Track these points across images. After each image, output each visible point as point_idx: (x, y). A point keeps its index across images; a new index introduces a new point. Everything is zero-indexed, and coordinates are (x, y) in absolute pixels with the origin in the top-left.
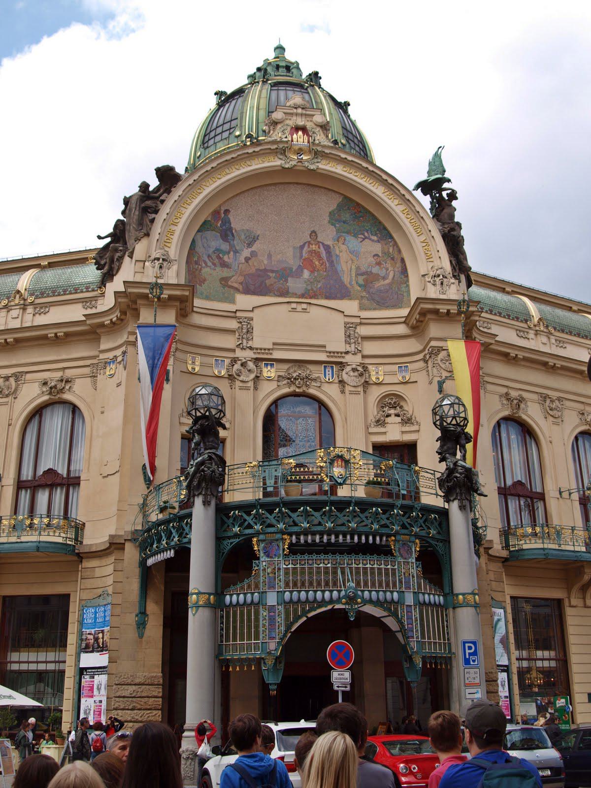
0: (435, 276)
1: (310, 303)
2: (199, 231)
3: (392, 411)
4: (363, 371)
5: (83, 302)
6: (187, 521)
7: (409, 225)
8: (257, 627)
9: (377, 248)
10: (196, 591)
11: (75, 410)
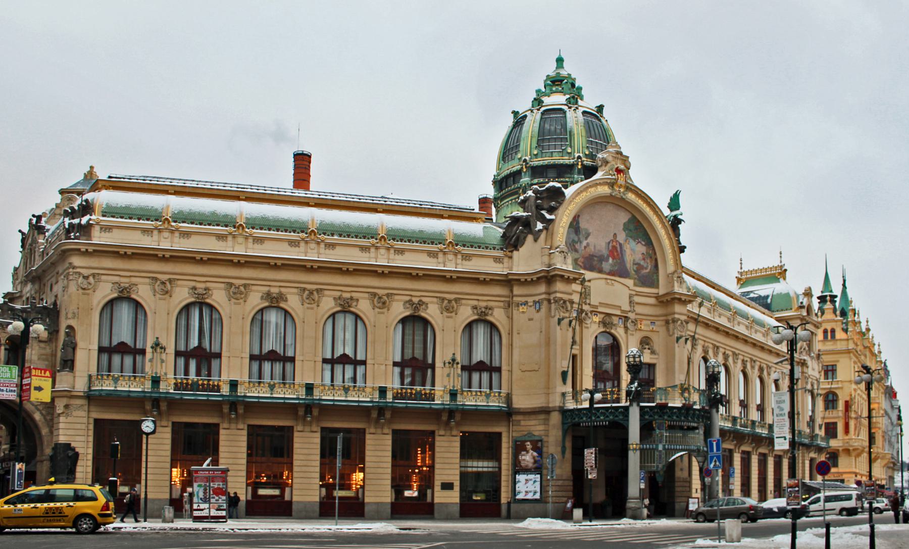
4: (635, 322)
11: (492, 326)
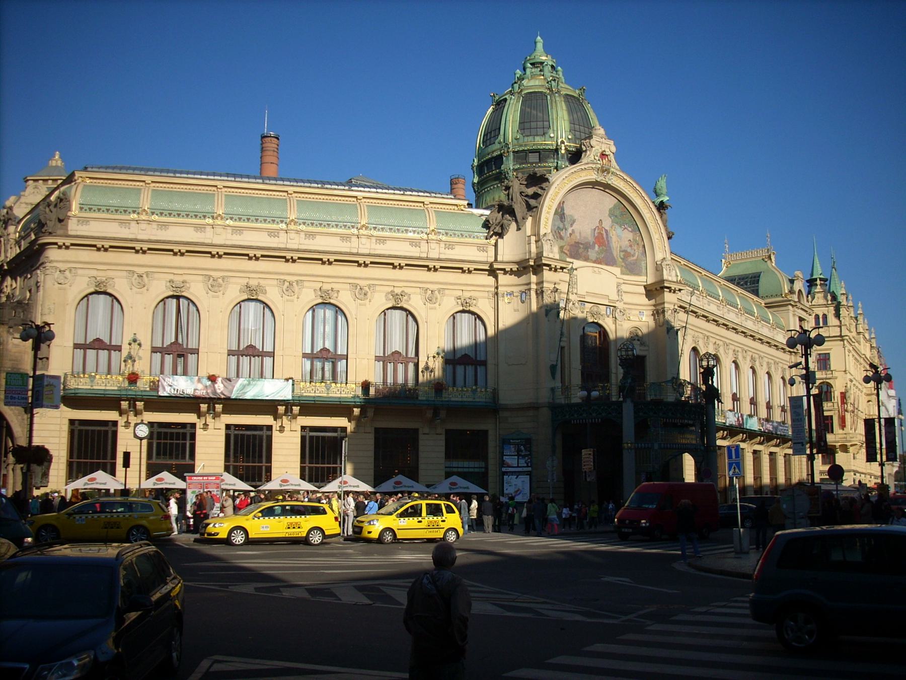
9: (630, 236)
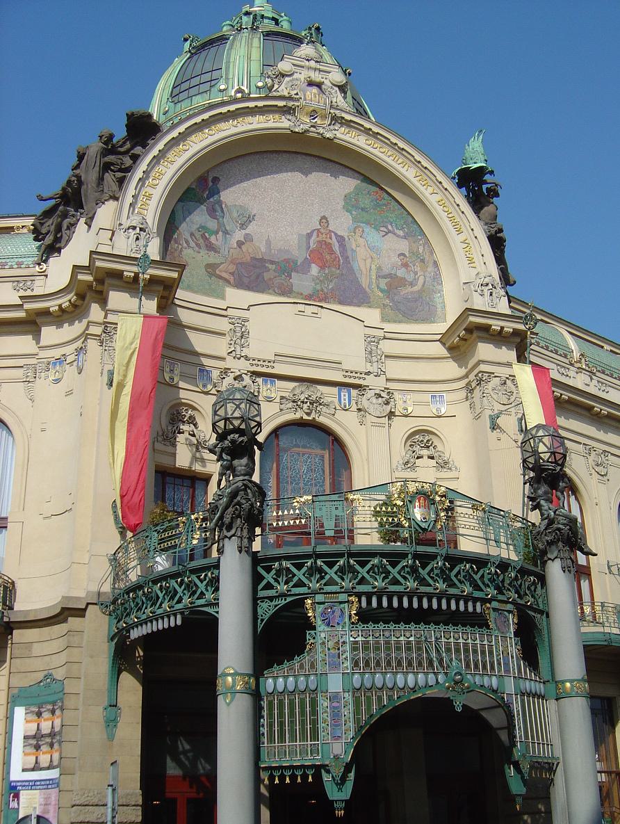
0: (482, 285)
1: (322, 307)
2: (180, 200)
3: (425, 452)
4: (386, 397)
5: (13, 282)
6: (206, 575)
7: (447, 220)
8: (314, 723)
9: (403, 246)
10: (232, 671)
